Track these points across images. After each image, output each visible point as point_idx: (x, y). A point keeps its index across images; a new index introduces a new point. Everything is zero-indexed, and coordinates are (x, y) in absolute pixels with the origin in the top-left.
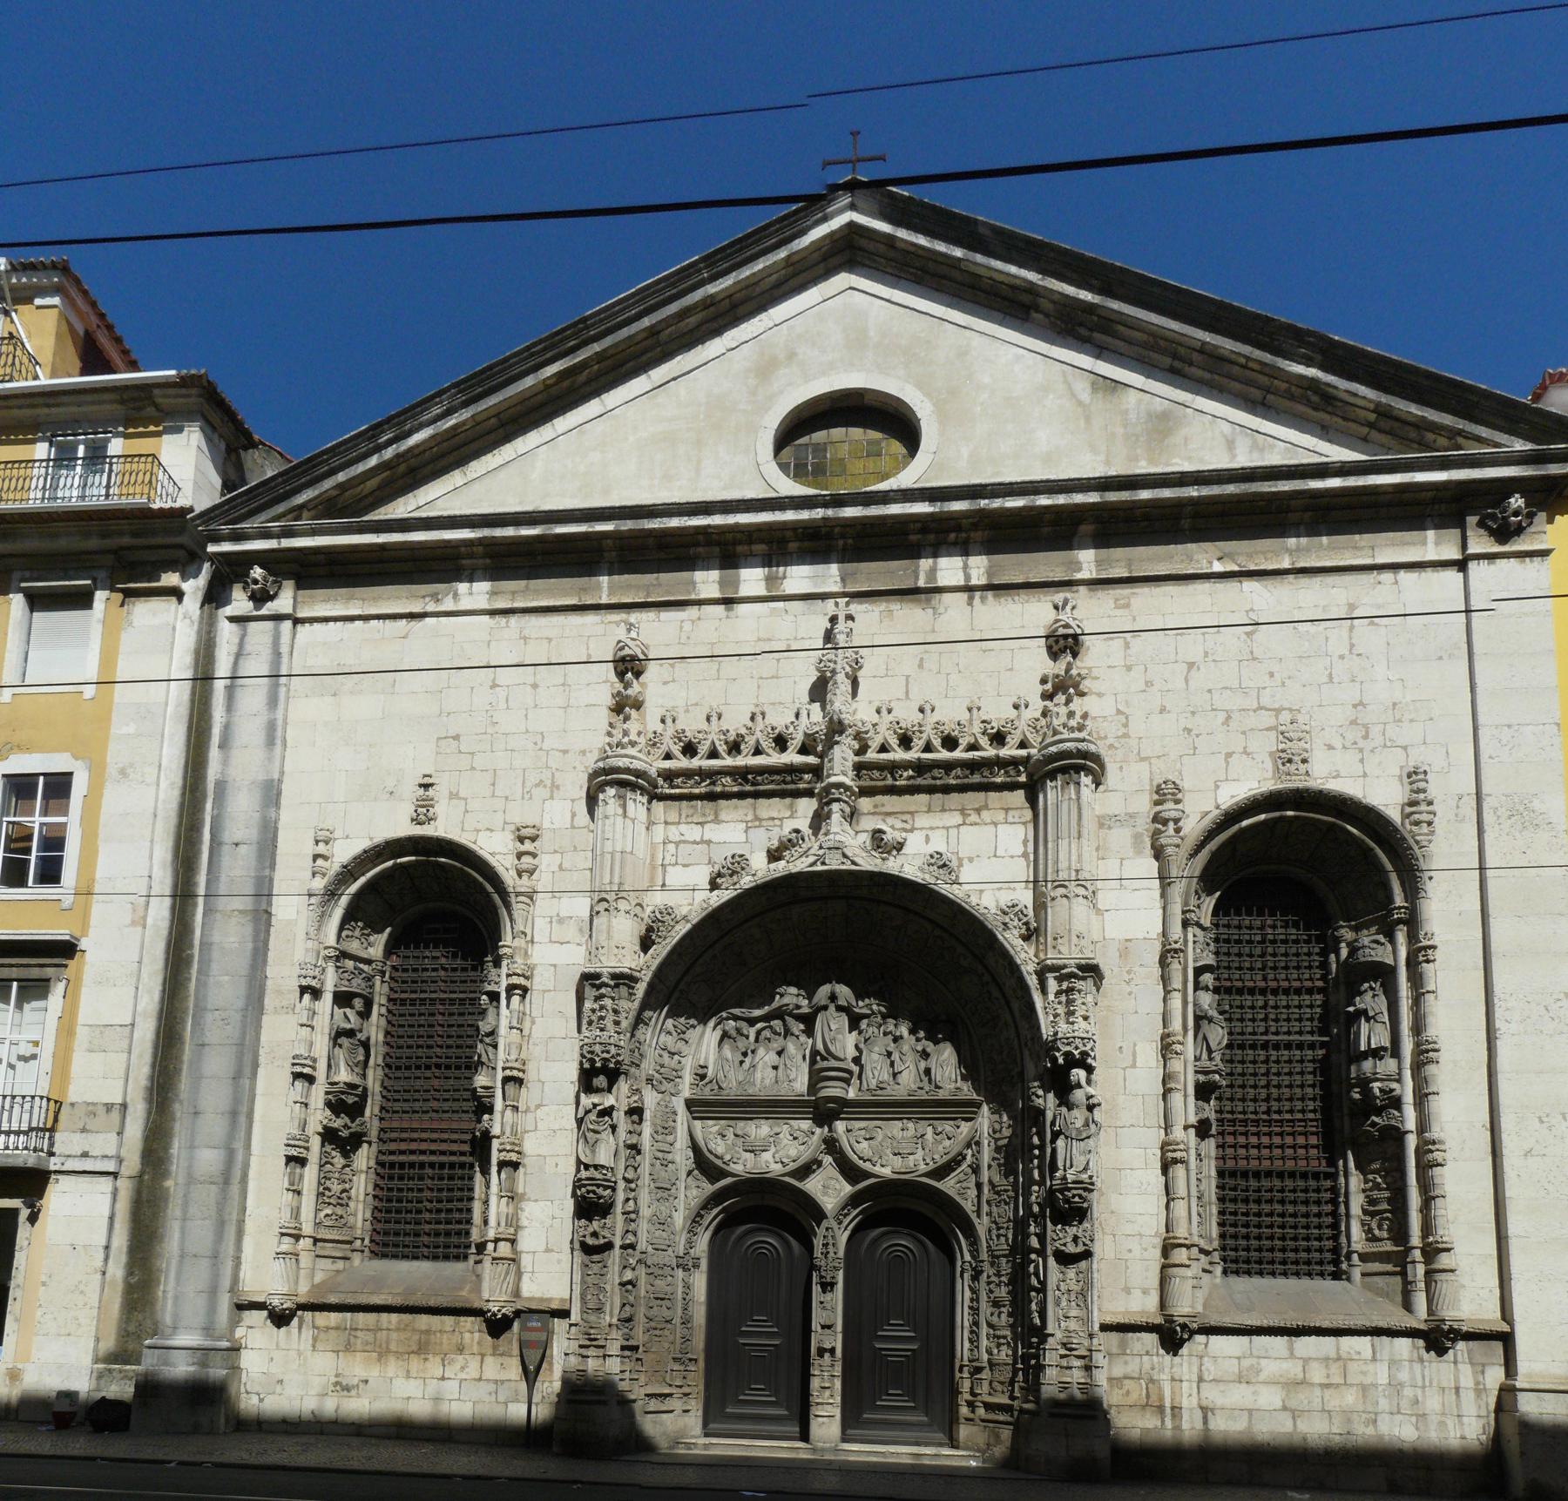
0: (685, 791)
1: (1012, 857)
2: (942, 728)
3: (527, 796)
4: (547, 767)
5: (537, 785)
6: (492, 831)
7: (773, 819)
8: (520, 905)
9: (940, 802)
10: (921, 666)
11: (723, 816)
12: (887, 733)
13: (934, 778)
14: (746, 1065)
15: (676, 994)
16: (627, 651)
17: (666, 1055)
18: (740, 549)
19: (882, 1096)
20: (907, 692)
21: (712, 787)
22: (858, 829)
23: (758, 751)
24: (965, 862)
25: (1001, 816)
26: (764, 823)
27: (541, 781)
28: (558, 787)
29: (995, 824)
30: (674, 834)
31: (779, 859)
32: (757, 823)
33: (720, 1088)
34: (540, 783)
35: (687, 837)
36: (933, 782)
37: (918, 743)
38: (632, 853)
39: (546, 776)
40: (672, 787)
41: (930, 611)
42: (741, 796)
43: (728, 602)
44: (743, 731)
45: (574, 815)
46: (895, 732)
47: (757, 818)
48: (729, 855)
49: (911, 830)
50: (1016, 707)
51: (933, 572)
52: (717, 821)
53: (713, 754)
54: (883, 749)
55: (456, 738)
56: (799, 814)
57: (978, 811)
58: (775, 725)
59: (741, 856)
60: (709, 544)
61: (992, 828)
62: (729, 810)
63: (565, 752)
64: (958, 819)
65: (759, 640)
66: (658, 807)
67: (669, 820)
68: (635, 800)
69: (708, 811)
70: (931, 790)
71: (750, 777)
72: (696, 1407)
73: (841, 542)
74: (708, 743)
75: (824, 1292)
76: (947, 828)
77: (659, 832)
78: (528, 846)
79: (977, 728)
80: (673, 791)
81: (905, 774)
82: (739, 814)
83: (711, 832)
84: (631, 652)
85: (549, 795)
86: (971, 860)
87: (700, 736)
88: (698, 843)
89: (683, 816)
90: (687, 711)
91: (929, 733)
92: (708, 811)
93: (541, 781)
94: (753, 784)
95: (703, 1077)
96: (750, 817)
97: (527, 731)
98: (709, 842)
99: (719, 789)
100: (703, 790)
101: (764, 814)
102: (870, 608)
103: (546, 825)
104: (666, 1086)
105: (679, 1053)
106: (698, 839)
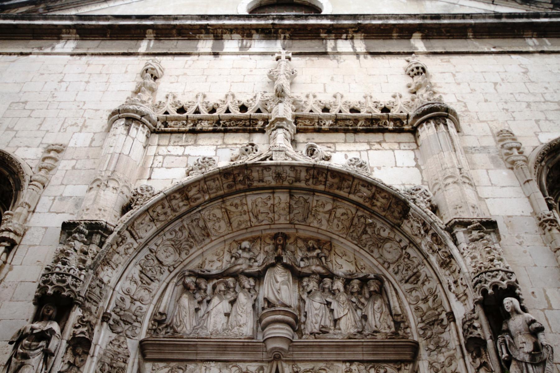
0: (176, 129)
1: (408, 167)
3: (62, 130)
4: (82, 117)
5: (72, 125)
6: (28, 147)
7: (236, 144)
8: (31, 187)
9: (353, 138)
10: (332, 79)
11: (200, 142)
12: (313, 106)
13: (348, 126)
14: (201, 313)
15: (146, 251)
16: (150, 66)
17: (128, 300)
19: (324, 339)
20: (325, 90)
21: (194, 127)
24: (375, 169)
25: (396, 146)
26: (230, 146)
27: (76, 123)
28: (86, 127)
29: (393, 150)
30: (163, 150)
32: (224, 146)
33: (175, 332)
34: (76, 124)
35: (172, 153)
36: (346, 127)
39: (80, 122)
40: (166, 127)
41: (335, 61)
42: (214, 131)
43: (216, 54)
44: (219, 102)
45: (93, 140)
46: (319, 105)
49: (335, 152)
50: (394, 97)
51: (335, 48)
52: (195, 144)
55: (25, 103)
57: (380, 143)
58: (240, 100)
61: (391, 152)
62: (203, 139)
63: (97, 110)
64: (367, 147)
65: (233, 68)
66: (155, 138)
67: (161, 144)
70: (346, 131)
71: (221, 122)
74: (195, 108)
76: (360, 151)
77: (152, 150)
78: (52, 154)
79: (371, 105)
80: (166, 129)
81: (327, 123)
83: (190, 150)
84: (152, 67)
85: (79, 130)
86: (379, 168)
87: (190, 104)
88: (180, 156)
91: (340, 105)
92: (190, 140)
93: (76, 123)
94: (223, 126)
95: (160, 322)
97: (75, 100)
98: (188, 156)
99: (198, 127)
100: (187, 128)
103: (71, 144)
104: (122, 327)
105: (141, 300)
106: (180, 154)
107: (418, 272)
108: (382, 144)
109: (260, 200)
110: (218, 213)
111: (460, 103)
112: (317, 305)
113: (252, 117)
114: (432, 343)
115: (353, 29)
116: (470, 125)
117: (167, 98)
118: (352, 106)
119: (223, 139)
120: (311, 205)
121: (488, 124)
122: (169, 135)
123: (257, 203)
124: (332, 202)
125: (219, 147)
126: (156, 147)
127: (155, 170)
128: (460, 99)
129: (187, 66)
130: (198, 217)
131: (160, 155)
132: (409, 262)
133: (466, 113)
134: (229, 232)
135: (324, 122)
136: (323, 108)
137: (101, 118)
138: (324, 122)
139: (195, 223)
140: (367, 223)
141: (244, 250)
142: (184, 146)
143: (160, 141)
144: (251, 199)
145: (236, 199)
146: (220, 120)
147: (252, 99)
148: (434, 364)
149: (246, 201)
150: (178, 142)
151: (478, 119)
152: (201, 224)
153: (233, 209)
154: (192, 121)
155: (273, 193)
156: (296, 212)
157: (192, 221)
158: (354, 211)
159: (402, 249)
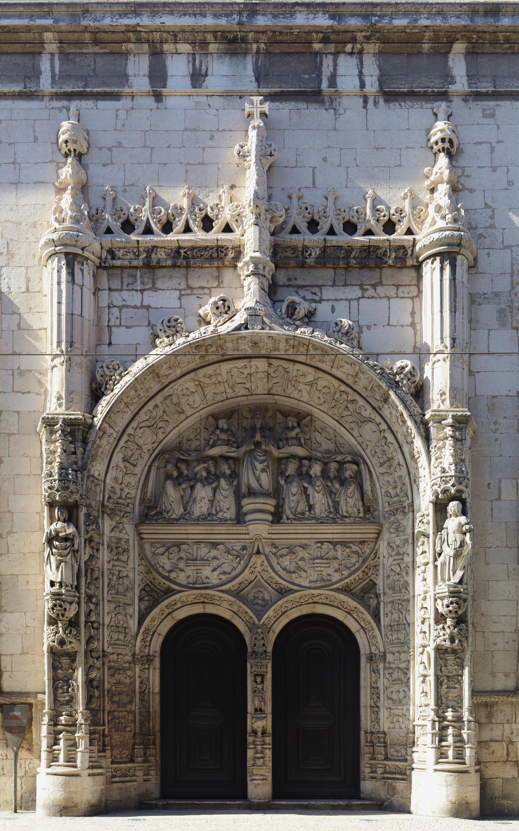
0: (126, 263)
2: (343, 215)
7: (203, 288)
11: (159, 284)
18: (166, 47)
22: (275, 299)
23: (187, 229)
26: (195, 292)
28: (13, 256)
31: (209, 323)
32: (189, 292)
35: (129, 303)
37: (324, 227)
38: (81, 315)
40: (113, 258)
41: (332, 111)
42: (174, 266)
45: (28, 281)
47: (189, 287)
48: (166, 319)
52: (154, 288)
53: (148, 231)
54: (295, 230)
56: (225, 284)
59: (176, 320)
60: (139, 41)
63: (19, 224)
65: (186, 130)
68: (82, 270)
69: (146, 280)
71: (182, 251)
72: (154, 779)
73: (255, 46)
75: (256, 682)
82: (174, 283)
89: (125, 284)
90: (125, 191)
96: (183, 286)
98: (148, 307)
101: (195, 283)
102: (281, 106)
107: (392, 458)
108: (377, 288)
109: (235, 369)
110: (191, 386)
111: (488, 210)
112: (294, 489)
113: (220, 243)
114: (393, 527)
115: (364, 34)
116: (489, 254)
117: (104, 199)
118: (347, 219)
119: (187, 278)
120: (291, 374)
121: (512, 251)
122: (118, 271)
123: (232, 373)
124: (313, 373)
125: (183, 292)
126: (107, 292)
127: (113, 328)
128: (489, 203)
129: (119, 124)
130: (170, 394)
131: (115, 306)
132: (385, 447)
133: (490, 231)
134: (205, 406)
135: (309, 252)
136: (309, 220)
137: (27, 238)
138: (309, 252)
139: (168, 401)
140: (349, 399)
141: (222, 430)
142: (142, 291)
143: (111, 282)
144: (225, 367)
145: (209, 370)
146: (180, 248)
147: (217, 205)
148: (392, 544)
149: (221, 371)
150: (132, 284)
151: (503, 242)
152: (175, 400)
153: (207, 380)
154: (145, 251)
155: (250, 362)
156: (275, 380)
157: (165, 399)
158: (336, 385)
159: (381, 432)
